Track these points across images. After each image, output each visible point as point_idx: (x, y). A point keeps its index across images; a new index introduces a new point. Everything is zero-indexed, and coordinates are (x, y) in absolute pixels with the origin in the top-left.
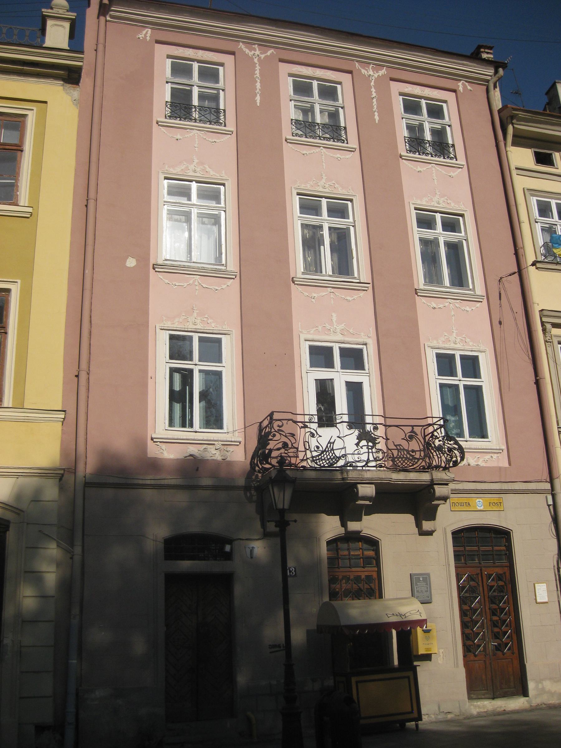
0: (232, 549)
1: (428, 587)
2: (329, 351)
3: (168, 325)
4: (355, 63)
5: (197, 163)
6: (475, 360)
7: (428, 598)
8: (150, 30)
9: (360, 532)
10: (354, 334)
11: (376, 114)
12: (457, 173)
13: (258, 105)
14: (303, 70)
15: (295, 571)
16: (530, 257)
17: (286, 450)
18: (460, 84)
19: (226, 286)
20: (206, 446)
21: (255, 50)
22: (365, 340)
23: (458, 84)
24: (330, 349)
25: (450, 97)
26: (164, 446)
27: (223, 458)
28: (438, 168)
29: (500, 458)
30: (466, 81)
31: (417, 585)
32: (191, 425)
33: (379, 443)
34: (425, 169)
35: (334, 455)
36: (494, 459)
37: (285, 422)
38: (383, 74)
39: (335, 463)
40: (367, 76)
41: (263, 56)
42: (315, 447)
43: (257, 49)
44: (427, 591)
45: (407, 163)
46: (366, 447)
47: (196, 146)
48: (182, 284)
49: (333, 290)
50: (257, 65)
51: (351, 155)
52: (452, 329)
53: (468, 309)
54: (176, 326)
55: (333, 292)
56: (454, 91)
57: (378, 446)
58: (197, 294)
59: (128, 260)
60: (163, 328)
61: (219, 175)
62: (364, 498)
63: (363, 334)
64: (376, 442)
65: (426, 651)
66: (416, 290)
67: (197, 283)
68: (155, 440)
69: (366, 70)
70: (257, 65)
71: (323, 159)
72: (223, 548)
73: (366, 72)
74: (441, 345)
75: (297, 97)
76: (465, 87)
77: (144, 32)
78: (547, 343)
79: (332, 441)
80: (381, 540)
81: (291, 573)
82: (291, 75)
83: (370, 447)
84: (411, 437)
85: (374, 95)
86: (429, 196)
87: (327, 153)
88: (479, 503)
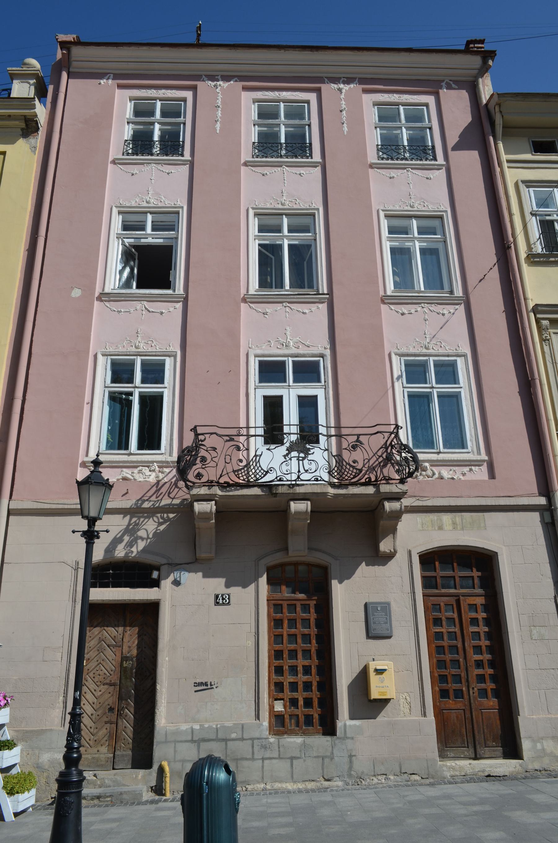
0: (159, 576)
1: (388, 618)
2: (281, 365)
3: (111, 350)
6: (453, 365)
7: (388, 631)
13: (218, 132)
15: (229, 599)
17: (203, 465)
20: (141, 467)
24: (283, 363)
30: (450, 80)
32: (127, 448)
35: (260, 469)
37: (207, 436)
43: (220, 79)
44: (386, 623)
46: (296, 458)
47: (153, 178)
48: (128, 310)
57: (310, 457)
63: (320, 346)
64: (310, 452)
65: (380, 695)
72: (151, 574)
74: (412, 351)
75: (261, 121)
78: (544, 343)
79: (259, 453)
80: (331, 564)
81: (224, 601)
82: (254, 101)
83: (300, 459)
84: (354, 447)
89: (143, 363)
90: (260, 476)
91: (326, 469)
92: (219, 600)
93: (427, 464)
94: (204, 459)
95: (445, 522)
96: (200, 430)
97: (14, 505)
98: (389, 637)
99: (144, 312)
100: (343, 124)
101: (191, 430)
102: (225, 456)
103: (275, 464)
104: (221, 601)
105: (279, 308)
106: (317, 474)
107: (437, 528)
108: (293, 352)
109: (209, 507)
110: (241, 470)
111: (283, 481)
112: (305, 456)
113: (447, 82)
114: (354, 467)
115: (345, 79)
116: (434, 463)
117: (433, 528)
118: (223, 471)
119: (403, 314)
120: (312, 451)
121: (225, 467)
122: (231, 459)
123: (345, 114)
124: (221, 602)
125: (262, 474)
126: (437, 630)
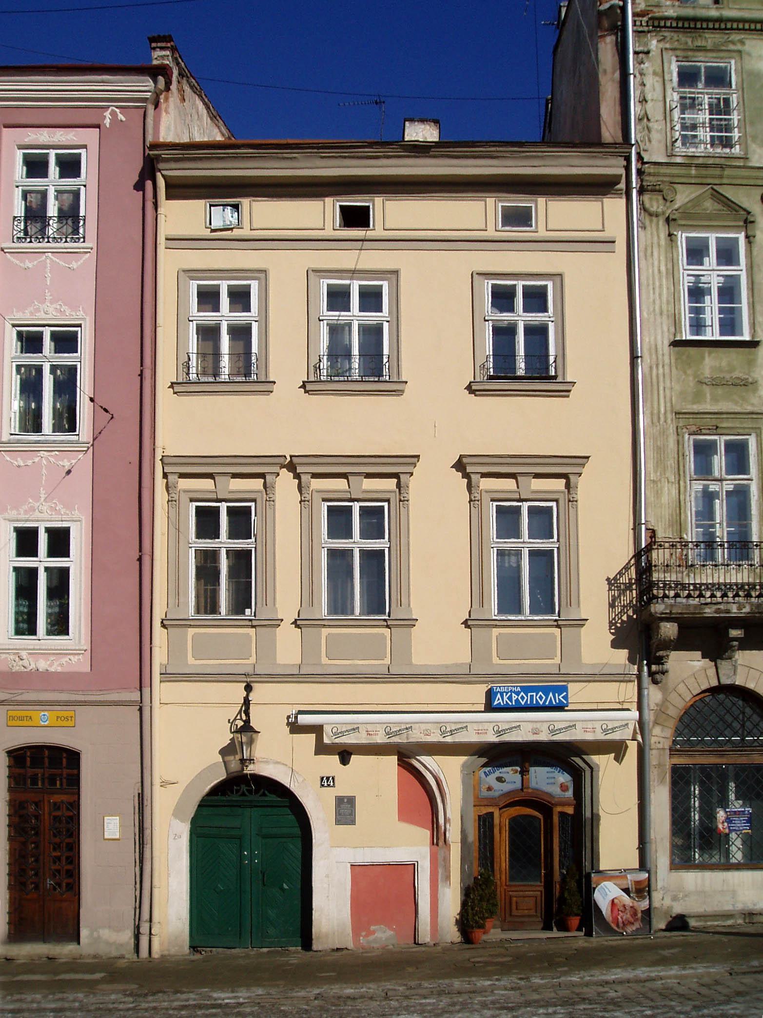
18: (107, 114)
30: (117, 107)
45: (12, 259)
88: (44, 716)
113: (112, 110)
119: (19, 466)
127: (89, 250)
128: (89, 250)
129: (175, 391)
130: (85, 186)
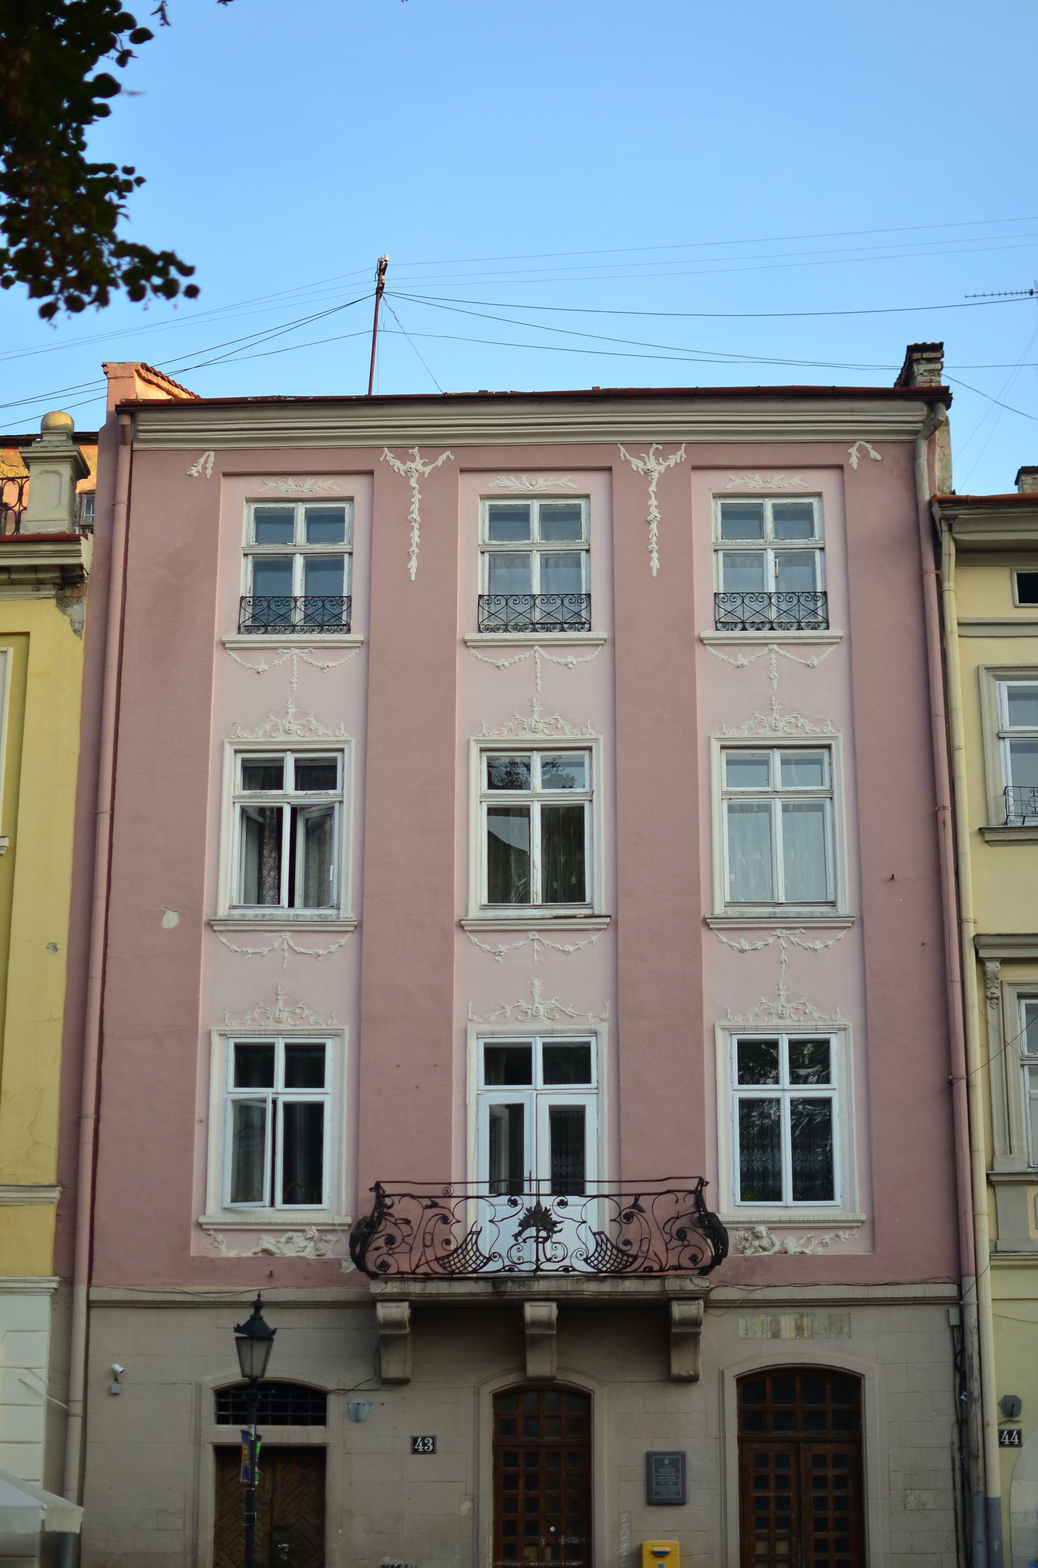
2: (523, 1053)
4: (619, 448)
5: (295, 715)
6: (823, 1047)
8: (212, 454)
9: (553, 1378)
10: (573, 1017)
11: (655, 555)
12: (826, 655)
13: (413, 578)
14: (511, 484)
15: (433, 1444)
16: (970, 818)
17: (390, 1249)
18: (853, 451)
19: (336, 946)
21: (413, 460)
22: (593, 1027)
23: (849, 451)
25: (823, 481)
26: (220, 1237)
27: (318, 1253)
28: (783, 652)
29: (856, 1237)
30: (868, 442)
31: (657, 1471)
33: (560, 1231)
34: (753, 658)
35: (478, 1254)
36: (844, 1240)
37: (396, 1199)
38: (678, 461)
39: (481, 1268)
40: (642, 474)
41: (428, 469)
42: (444, 1243)
44: (676, 1484)
46: (533, 1239)
47: (294, 680)
48: (259, 950)
49: (537, 936)
50: (416, 492)
51: (597, 653)
52: (778, 989)
53: (818, 945)
54: (249, 1026)
55: (538, 940)
56: (840, 467)
57: (556, 1237)
58: (285, 965)
59: (165, 917)
60: (223, 1033)
61: (331, 734)
62: (537, 1323)
63: (591, 1014)
64: (555, 1229)
66: (705, 919)
67: (286, 947)
68: (204, 1227)
69: (642, 459)
70: (416, 492)
71: (538, 670)
73: (640, 464)
74: (752, 1022)
76: (863, 454)
77: (202, 461)
78: (988, 1002)
81: (426, 1447)
83: (541, 1240)
84: (629, 1217)
85: (654, 512)
86: (758, 715)
87: (547, 657)
89: (289, 1048)
90: (478, 1265)
91: (581, 1255)
92: (418, 1446)
93: (762, 1229)
94: (390, 1240)
95: (784, 1325)
96: (388, 1189)
97: (96, 1294)
98: (681, 1502)
99: (286, 954)
100: (651, 552)
101: (371, 1189)
102: (424, 1234)
103: (502, 1248)
104: (421, 1448)
105: (521, 943)
106: (566, 1262)
107: (769, 1336)
108: (544, 1028)
109: (401, 1311)
110: (452, 1254)
111: (513, 1271)
112: (548, 1234)
113: (860, 445)
114: (624, 1253)
115: (660, 447)
116: (775, 1226)
117: (765, 1336)
118: (420, 1260)
119: (743, 951)
120: (559, 1227)
121: (424, 1253)
122: (432, 1240)
123: (655, 531)
124: (421, 1450)
125: (482, 1262)
126: (759, 1494)
127: (838, 640)
128: (838, 640)
129: (987, 839)
130: (822, 549)
